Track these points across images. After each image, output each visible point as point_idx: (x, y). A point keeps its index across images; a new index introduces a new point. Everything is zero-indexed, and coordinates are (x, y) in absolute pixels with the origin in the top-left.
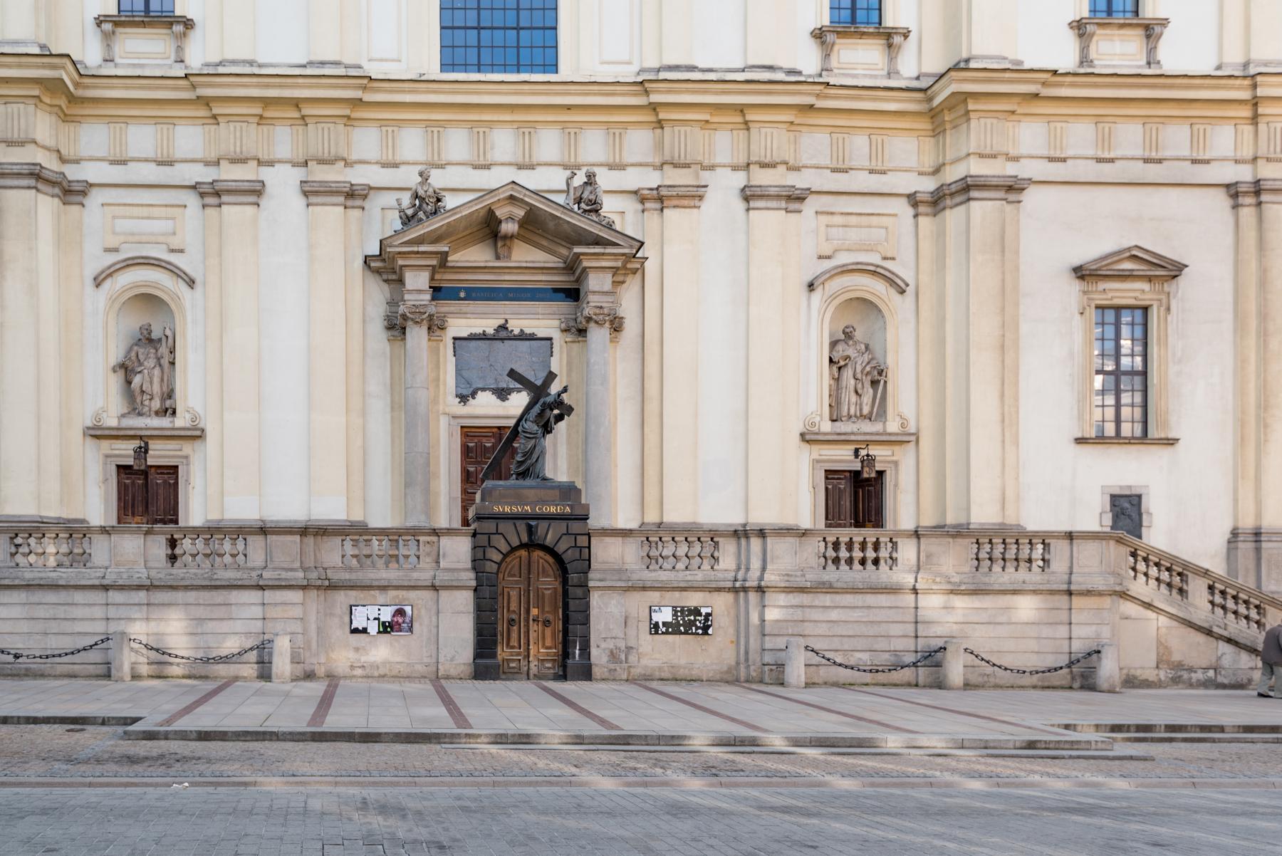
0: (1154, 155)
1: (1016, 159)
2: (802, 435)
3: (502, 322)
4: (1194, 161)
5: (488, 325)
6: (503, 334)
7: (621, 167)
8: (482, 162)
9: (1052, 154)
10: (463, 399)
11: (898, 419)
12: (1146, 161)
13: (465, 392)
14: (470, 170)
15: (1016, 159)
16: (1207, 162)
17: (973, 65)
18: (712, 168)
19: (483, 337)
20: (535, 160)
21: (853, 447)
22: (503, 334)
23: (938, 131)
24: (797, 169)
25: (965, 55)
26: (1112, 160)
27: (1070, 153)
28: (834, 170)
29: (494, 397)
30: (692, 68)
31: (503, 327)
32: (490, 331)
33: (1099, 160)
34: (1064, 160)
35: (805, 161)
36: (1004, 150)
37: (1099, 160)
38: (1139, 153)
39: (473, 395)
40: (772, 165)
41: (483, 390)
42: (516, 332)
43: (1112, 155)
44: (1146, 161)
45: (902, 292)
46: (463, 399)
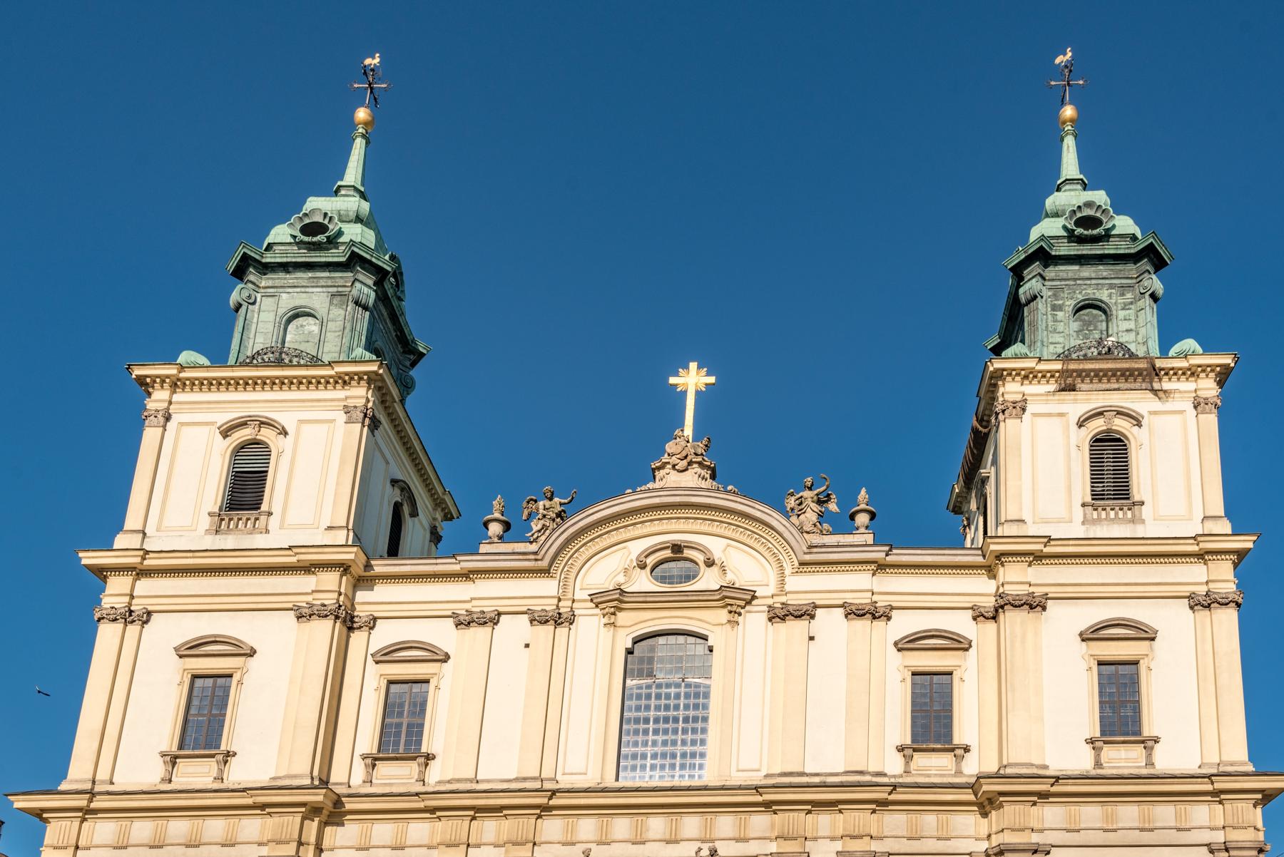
0: (1147, 826)
1: (1042, 831)
4: (1179, 830)
7: (746, 840)
8: (639, 839)
9: (1068, 826)
12: (1142, 830)
14: (630, 845)
15: (1042, 831)
16: (1189, 830)
17: (1009, 771)
18: (815, 839)
20: (679, 838)
23: (985, 815)
24: (881, 838)
25: (1005, 763)
26: (1115, 830)
27: (1083, 826)
28: (909, 839)
30: (802, 774)
33: (1106, 830)
34: (1078, 831)
35: (886, 834)
36: (1031, 825)
37: (1106, 830)
38: (1136, 825)
40: (861, 837)
43: (1115, 827)
44: (1142, 830)
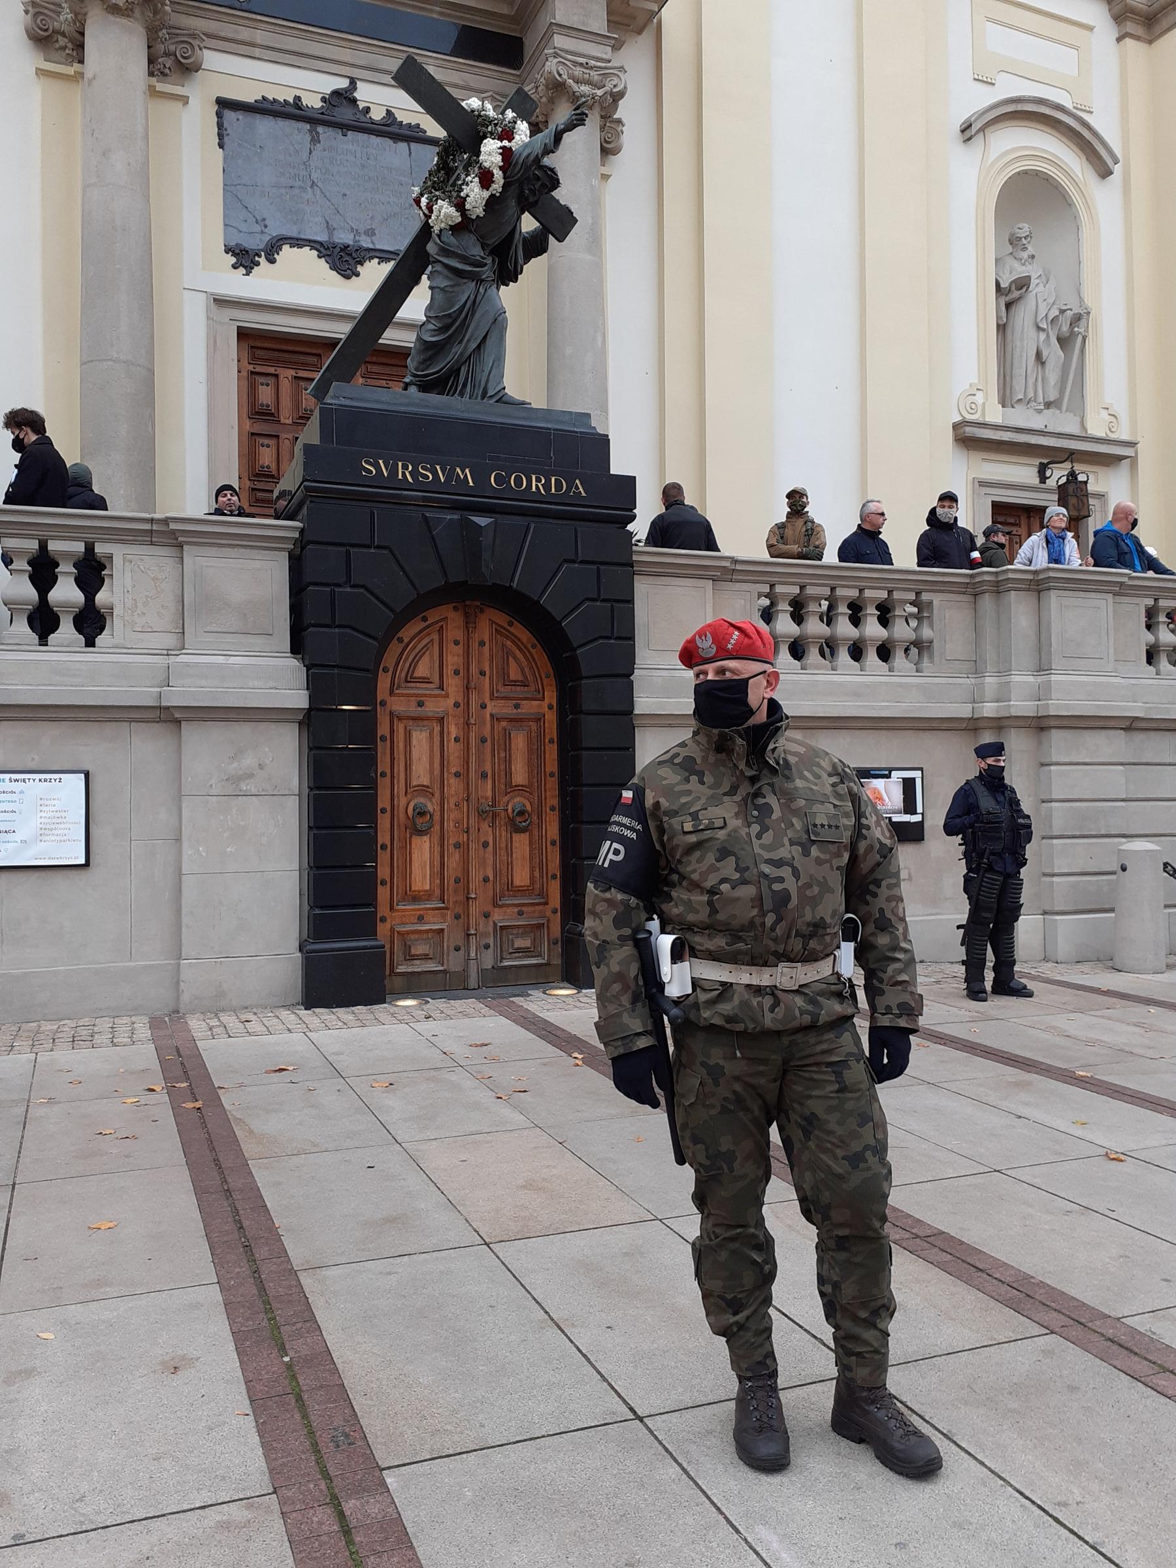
2: (956, 426)
3: (343, 83)
5: (312, 86)
6: (344, 114)
10: (245, 259)
11: (1104, 414)
13: (254, 242)
19: (292, 111)
21: (1037, 462)
22: (344, 114)
29: (323, 264)
31: (343, 97)
32: (313, 102)
39: (271, 251)
41: (297, 243)
42: (377, 115)
45: (1105, 173)
46: (245, 259)
